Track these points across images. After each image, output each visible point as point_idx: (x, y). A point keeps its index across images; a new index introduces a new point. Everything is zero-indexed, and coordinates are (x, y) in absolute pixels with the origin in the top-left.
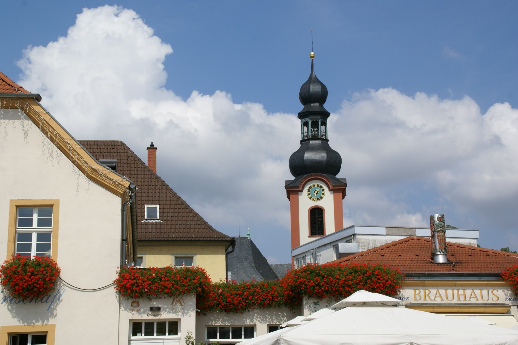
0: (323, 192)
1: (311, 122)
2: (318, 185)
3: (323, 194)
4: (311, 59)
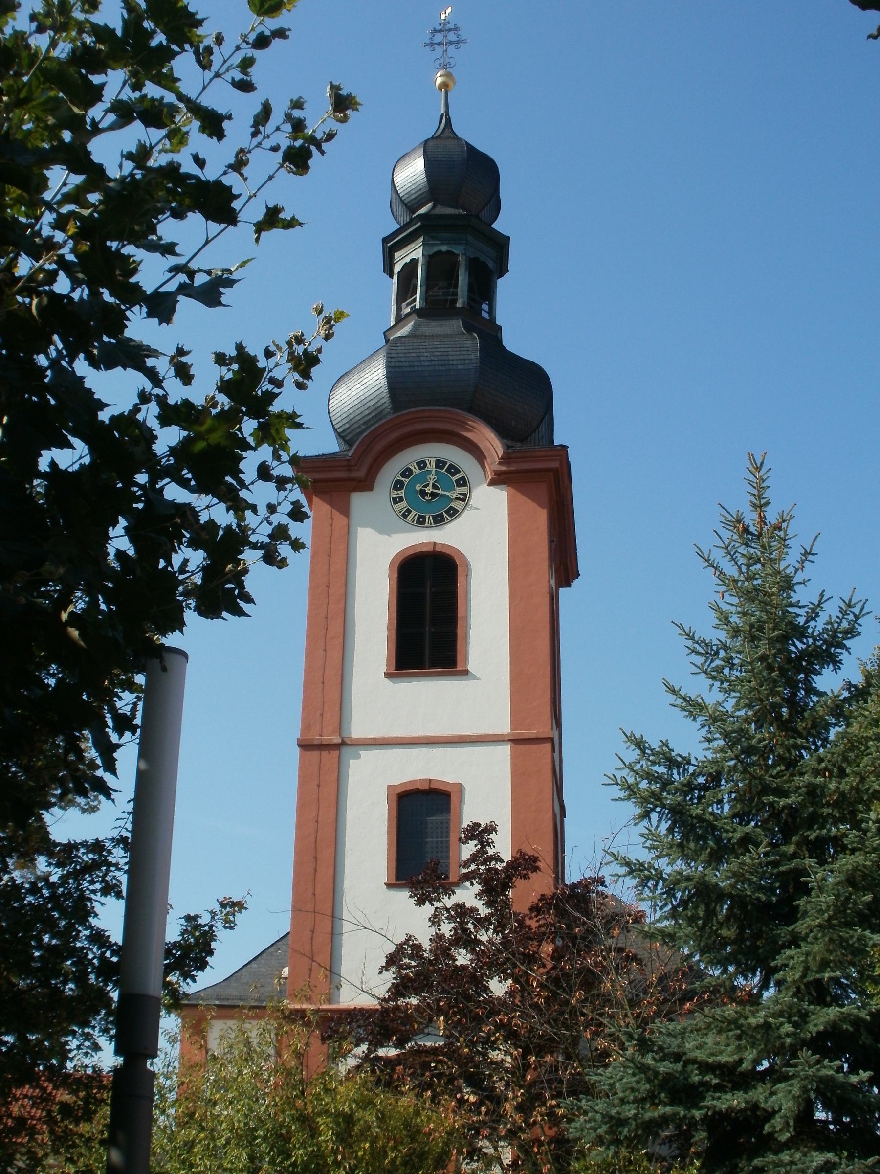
2: (440, 464)
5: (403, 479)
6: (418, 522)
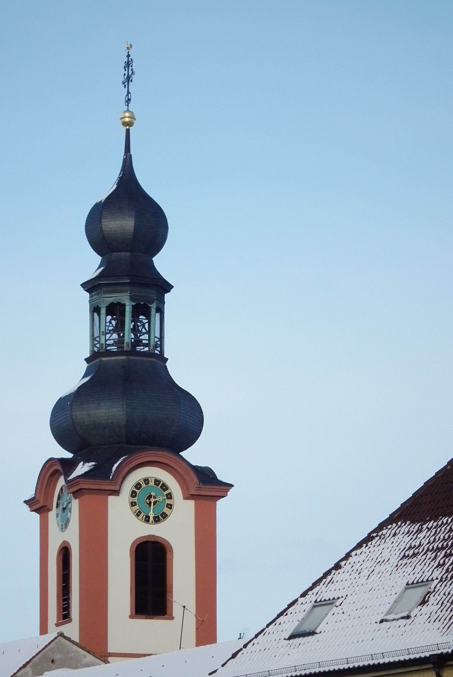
0: (169, 501)
1: (133, 305)
2: (157, 482)
3: (170, 506)
4: (124, 129)
5: (137, 491)
6: (145, 520)
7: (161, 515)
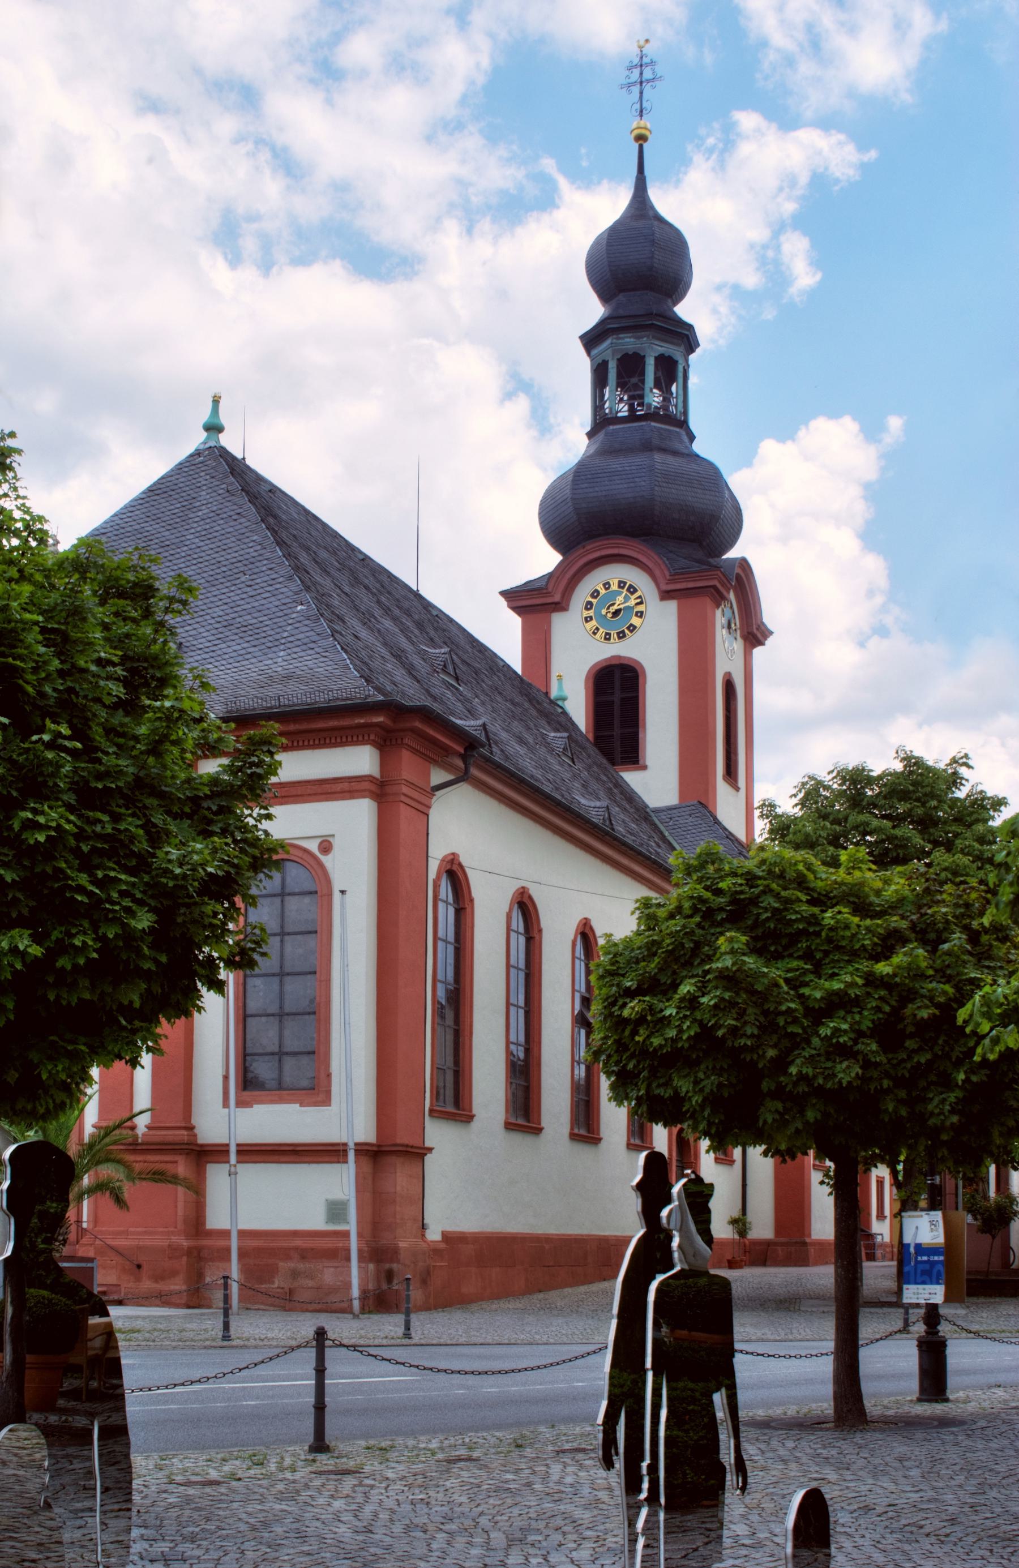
4: (636, 146)
6: (606, 639)
7: (628, 628)
